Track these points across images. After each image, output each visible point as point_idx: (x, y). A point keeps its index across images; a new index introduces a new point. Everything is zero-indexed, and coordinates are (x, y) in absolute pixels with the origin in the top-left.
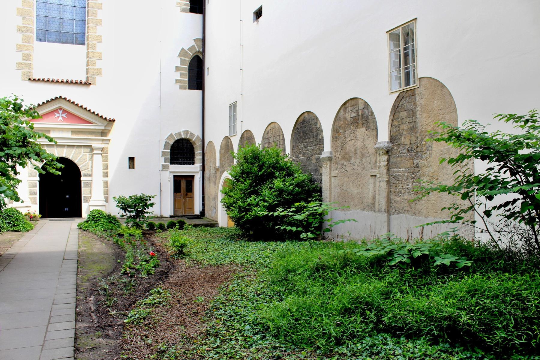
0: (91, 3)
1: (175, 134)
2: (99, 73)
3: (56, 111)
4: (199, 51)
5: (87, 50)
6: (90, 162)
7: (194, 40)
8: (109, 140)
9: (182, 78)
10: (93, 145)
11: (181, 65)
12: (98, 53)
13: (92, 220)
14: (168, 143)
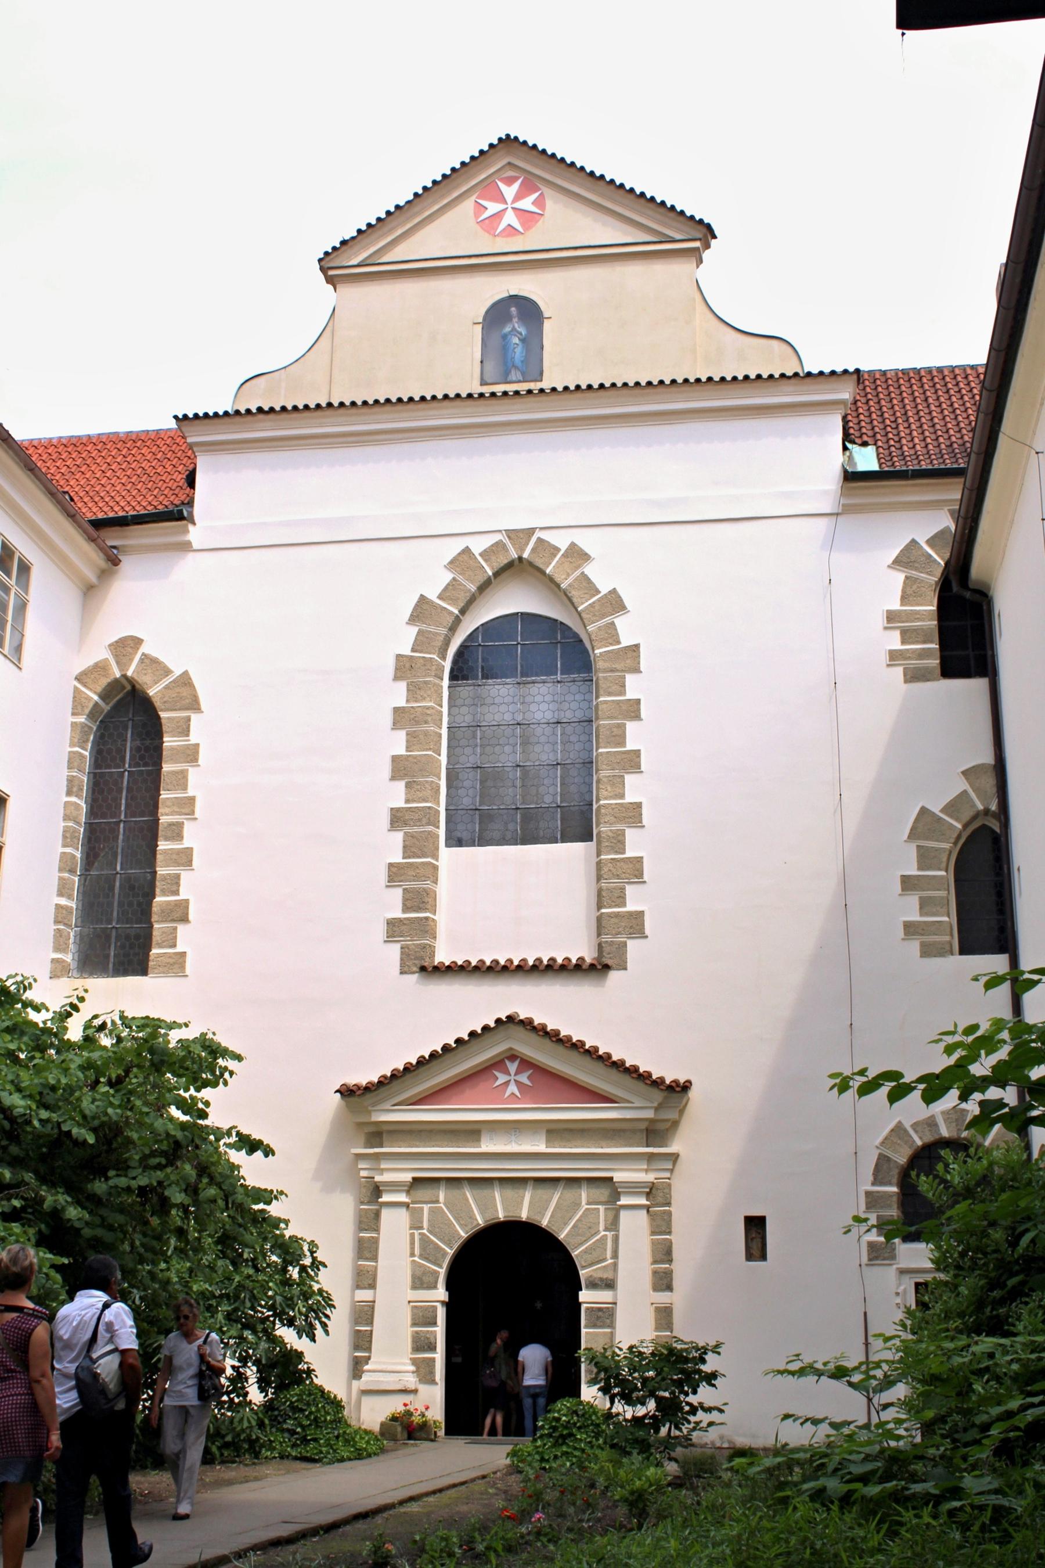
0: (606, 702)
1: (915, 1126)
2: (635, 924)
3: (497, 1064)
4: (987, 812)
5: (598, 854)
6: (610, 1234)
7: (964, 773)
8: (675, 1157)
9: (927, 914)
10: (618, 1176)
11: (920, 868)
12: (630, 860)
13: (550, 1435)
14: (888, 1159)
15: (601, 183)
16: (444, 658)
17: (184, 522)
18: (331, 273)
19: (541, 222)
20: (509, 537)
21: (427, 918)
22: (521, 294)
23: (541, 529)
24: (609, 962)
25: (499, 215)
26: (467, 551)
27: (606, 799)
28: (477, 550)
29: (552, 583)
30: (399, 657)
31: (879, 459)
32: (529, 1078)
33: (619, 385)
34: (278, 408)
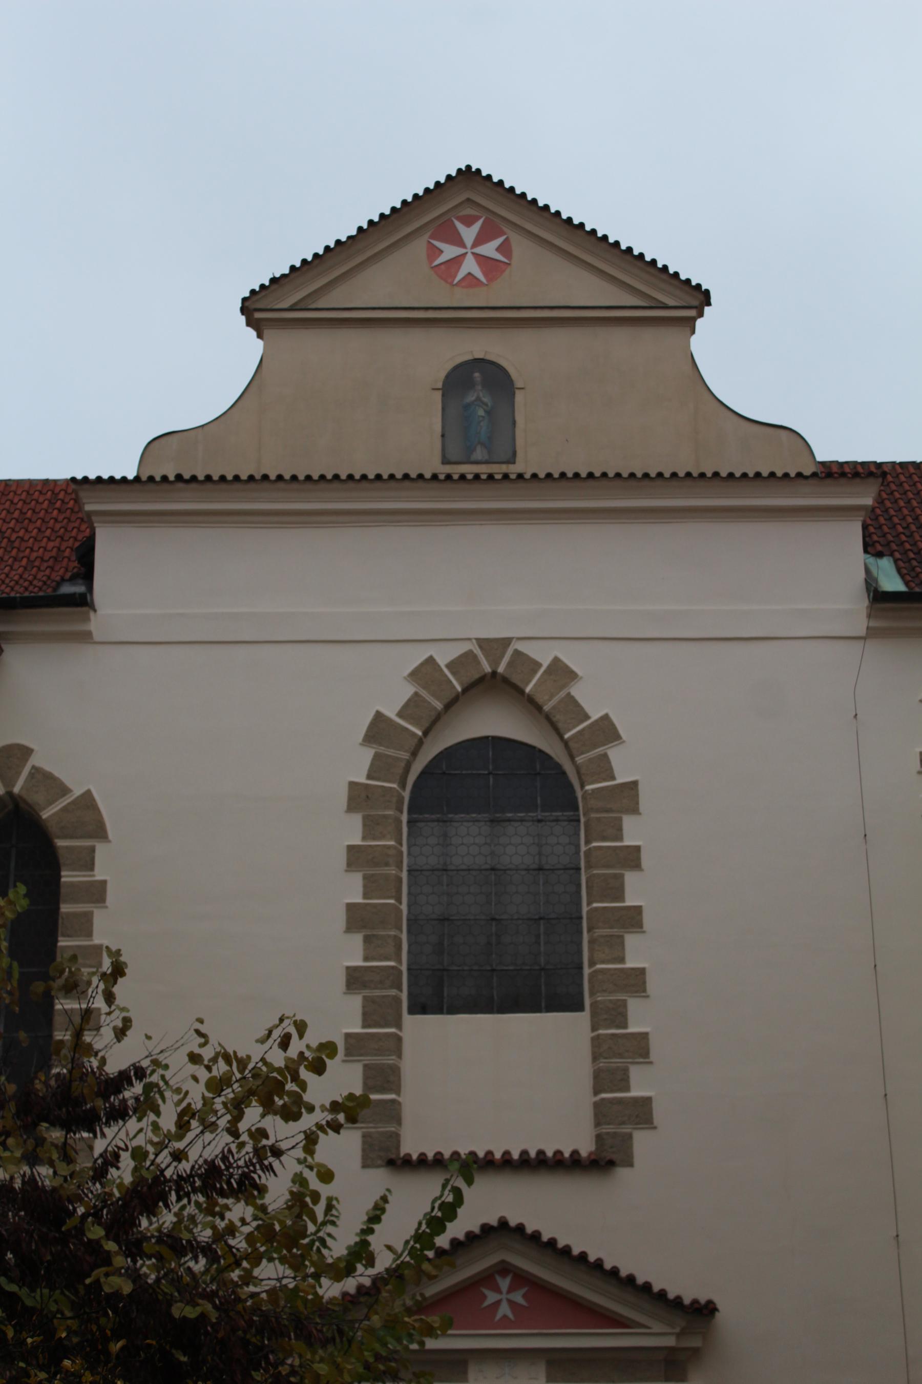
15: (579, 232)
16: (403, 785)
17: (85, 609)
18: (258, 315)
19: (507, 272)
20: (481, 647)
21: (393, 1101)
22: (489, 357)
23: (519, 639)
24: (614, 1157)
25: (458, 260)
26: (431, 661)
27: (603, 962)
28: (442, 662)
29: (532, 704)
30: (352, 785)
31: (902, 576)
32: (525, 1296)
33: (611, 475)
34: (201, 477)
